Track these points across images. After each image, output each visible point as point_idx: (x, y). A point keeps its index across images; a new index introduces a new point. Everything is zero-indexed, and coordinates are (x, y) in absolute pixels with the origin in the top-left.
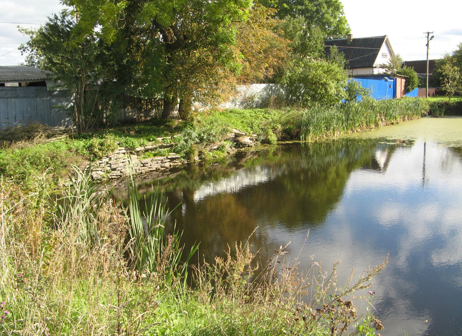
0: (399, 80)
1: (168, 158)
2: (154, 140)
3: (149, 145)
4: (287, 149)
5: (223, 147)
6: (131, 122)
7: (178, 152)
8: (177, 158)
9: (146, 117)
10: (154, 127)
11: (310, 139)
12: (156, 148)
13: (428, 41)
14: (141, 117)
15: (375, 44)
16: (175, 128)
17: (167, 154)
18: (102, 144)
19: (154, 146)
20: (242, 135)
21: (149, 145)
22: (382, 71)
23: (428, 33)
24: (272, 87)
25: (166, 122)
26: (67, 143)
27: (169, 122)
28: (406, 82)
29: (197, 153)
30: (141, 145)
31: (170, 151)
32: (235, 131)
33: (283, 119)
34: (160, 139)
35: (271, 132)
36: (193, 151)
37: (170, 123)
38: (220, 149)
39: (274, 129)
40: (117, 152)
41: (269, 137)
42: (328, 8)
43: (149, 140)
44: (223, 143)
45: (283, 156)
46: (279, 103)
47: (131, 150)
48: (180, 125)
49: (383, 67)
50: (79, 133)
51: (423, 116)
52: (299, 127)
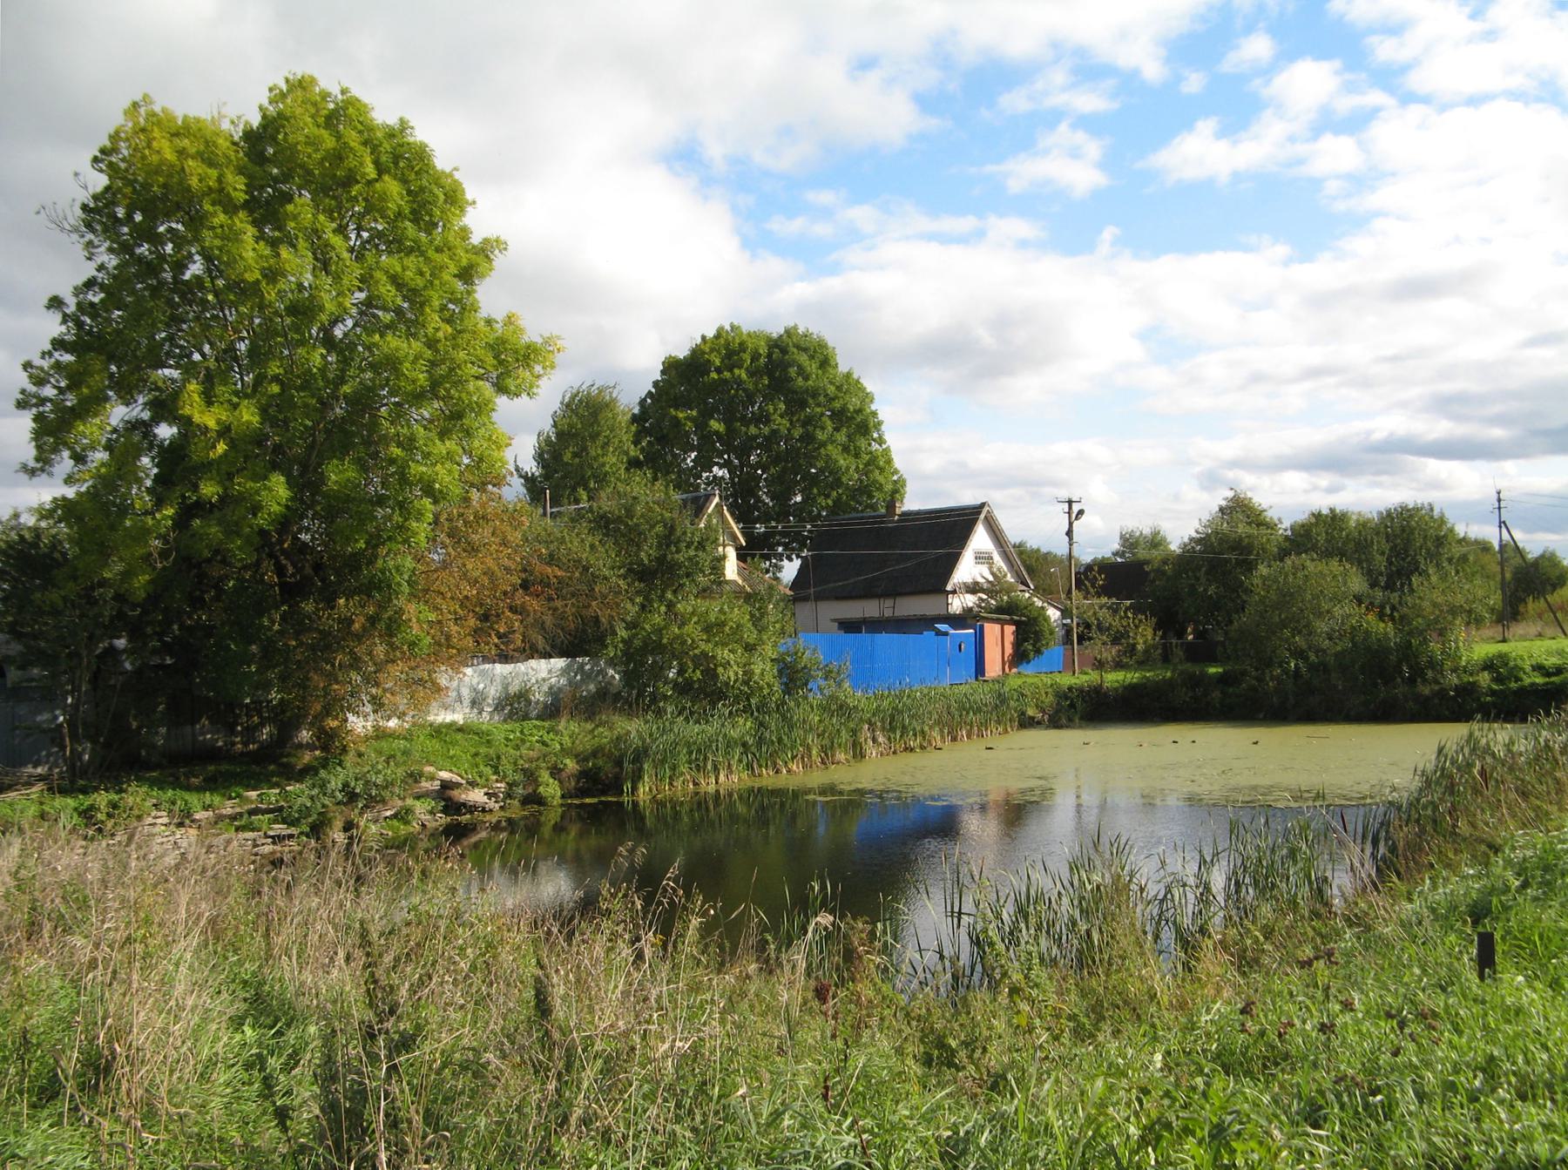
0: (992, 631)
1: (267, 836)
2: (239, 796)
3: (229, 808)
4: (593, 817)
5: (409, 811)
6: (210, 755)
7: (292, 823)
8: (291, 836)
9: (246, 744)
10: (257, 769)
11: (644, 792)
12: (241, 815)
13: (1071, 524)
14: (234, 744)
15: (953, 526)
16: (302, 771)
17: (265, 827)
18: (115, 806)
19: (238, 810)
20: (458, 785)
21: (229, 808)
22: (970, 600)
23: (1070, 502)
24: (582, 665)
25: (282, 755)
26: (42, 803)
27: (289, 755)
28: (1017, 633)
29: (338, 824)
30: (206, 808)
31: (275, 821)
32: (445, 775)
33: (586, 744)
34: (253, 794)
35: (545, 776)
36: (330, 821)
37: (293, 760)
38: (403, 816)
39: (556, 772)
40: (150, 820)
41: (541, 789)
42: (837, 429)
43: (230, 798)
44: (409, 802)
45: (582, 835)
46: (590, 706)
47: (184, 819)
48: (315, 763)
49: (973, 588)
50: (72, 782)
51: (1026, 723)
52: (619, 763)
